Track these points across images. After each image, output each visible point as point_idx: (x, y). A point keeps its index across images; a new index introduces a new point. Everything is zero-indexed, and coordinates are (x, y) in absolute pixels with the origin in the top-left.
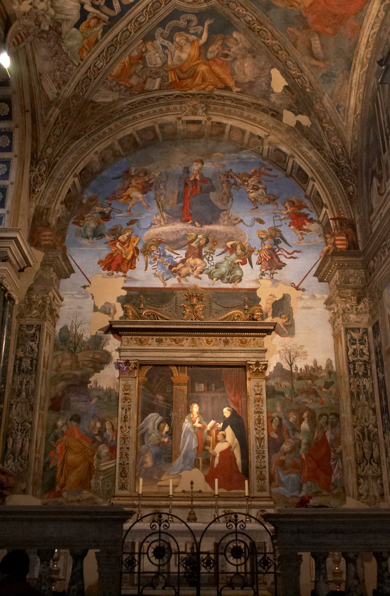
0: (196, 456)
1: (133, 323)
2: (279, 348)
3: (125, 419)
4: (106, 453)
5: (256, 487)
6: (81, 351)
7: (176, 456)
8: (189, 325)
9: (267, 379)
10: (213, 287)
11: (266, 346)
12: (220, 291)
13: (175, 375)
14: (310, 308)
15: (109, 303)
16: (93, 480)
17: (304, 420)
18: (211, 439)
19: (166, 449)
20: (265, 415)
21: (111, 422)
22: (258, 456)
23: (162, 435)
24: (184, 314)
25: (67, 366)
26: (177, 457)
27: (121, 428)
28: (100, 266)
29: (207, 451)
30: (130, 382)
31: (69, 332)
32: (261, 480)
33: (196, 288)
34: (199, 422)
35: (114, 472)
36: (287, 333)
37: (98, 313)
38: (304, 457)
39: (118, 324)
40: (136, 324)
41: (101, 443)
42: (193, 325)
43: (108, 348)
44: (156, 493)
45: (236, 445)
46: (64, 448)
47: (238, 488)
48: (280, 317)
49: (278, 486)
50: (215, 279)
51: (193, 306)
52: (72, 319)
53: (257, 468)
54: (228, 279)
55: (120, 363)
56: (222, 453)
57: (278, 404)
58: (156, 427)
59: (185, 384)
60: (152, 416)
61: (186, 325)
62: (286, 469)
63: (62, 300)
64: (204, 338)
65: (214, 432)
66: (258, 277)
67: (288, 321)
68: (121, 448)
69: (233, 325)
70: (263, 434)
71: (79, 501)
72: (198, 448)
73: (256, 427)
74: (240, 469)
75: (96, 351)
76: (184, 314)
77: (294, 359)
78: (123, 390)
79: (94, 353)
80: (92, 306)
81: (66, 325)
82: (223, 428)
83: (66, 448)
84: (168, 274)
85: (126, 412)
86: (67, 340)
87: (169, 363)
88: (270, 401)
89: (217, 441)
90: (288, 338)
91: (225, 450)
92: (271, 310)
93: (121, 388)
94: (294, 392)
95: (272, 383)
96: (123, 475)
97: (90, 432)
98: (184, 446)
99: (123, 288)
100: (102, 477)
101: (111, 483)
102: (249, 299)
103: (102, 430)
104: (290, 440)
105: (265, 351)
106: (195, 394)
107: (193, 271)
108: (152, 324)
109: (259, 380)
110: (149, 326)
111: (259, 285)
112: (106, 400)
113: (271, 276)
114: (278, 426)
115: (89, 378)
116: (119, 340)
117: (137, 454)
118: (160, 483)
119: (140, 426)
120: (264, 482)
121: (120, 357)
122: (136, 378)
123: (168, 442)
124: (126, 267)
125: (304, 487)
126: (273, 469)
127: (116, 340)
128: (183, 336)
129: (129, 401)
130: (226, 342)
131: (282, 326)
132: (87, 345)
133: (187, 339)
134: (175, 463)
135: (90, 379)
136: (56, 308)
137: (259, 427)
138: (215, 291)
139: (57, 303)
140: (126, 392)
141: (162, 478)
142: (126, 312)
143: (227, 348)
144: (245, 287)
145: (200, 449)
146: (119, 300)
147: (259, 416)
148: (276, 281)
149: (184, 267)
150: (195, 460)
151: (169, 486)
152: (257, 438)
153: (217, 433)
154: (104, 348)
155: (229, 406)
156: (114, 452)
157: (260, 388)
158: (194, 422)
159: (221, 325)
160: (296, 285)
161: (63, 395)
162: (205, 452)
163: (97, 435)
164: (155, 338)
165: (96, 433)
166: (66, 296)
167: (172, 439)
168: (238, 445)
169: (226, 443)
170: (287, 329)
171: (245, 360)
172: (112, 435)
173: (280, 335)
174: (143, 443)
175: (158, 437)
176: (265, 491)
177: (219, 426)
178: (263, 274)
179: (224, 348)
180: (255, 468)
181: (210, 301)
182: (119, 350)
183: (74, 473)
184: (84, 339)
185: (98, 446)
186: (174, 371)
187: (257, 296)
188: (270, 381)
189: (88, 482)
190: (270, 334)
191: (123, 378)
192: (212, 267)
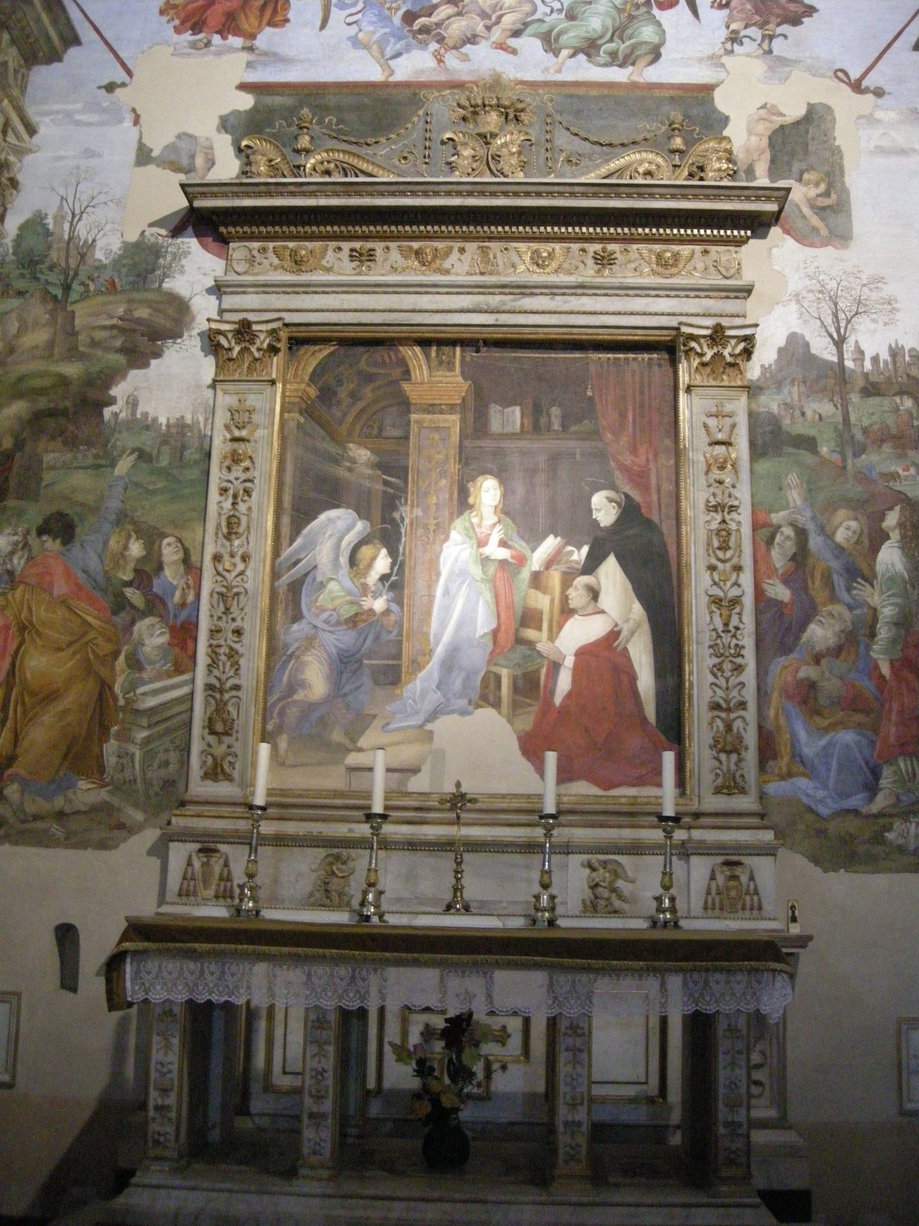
0: (489, 662)
1: (268, 190)
2: (796, 282)
3: (231, 527)
4: (160, 647)
5: (708, 779)
6: (86, 295)
7: (414, 661)
8: (470, 194)
9: (752, 390)
10: (560, 77)
11: (747, 277)
12: (581, 91)
13: (416, 374)
14: (903, 152)
15: (190, 136)
16: (112, 741)
17: (884, 536)
18: (543, 602)
19: (377, 637)
20: (743, 519)
21: (180, 540)
22: (719, 667)
23: (365, 587)
24: (451, 167)
25: (37, 347)
26: (417, 666)
27: (217, 558)
28: (164, 19)
29: (531, 644)
30: (252, 400)
31: (48, 233)
32: (728, 753)
33: (496, 83)
34: (503, 544)
35: (185, 716)
36: (824, 232)
37: (152, 168)
38: (885, 670)
39: (215, 195)
40: (281, 194)
41: (144, 614)
42: (482, 194)
43: (177, 284)
44: (336, 794)
45: (638, 626)
46: (14, 630)
47: (640, 782)
48: (800, 180)
49: (790, 775)
50: (565, 53)
51: (485, 139)
52: (62, 192)
53: (716, 706)
54: (613, 55)
55: (219, 332)
56: (583, 654)
57: (793, 478)
58: (344, 560)
59: (452, 408)
60: (330, 520)
61: (459, 194)
62: (818, 712)
63: (32, 130)
64: (522, 246)
65: (555, 579)
66: (718, 49)
67: (827, 194)
68: (215, 632)
69: (629, 196)
70: (736, 584)
71: (61, 815)
72: (495, 633)
73: (714, 561)
74: (650, 711)
75: (136, 295)
76: (451, 167)
77: (848, 322)
78: (227, 427)
79: (130, 301)
80: (134, 146)
81: (39, 212)
82: (591, 565)
83: (22, 628)
84: (400, 38)
85: (234, 504)
86: (43, 262)
87: (393, 333)
88: (764, 466)
89: (567, 611)
90: (829, 250)
91: (597, 644)
92: (767, 155)
93: (222, 418)
94: (853, 437)
95: (771, 403)
96: (219, 727)
97: (109, 580)
98: (443, 625)
99: (244, 87)
100: (144, 734)
101: (173, 757)
102: (686, 116)
103: (146, 569)
104: (837, 608)
105: (747, 291)
106: (487, 444)
107: (488, 28)
108: (337, 194)
109: (725, 392)
110: (323, 202)
111: (722, 75)
112: (164, 462)
113: (765, 46)
114: (793, 558)
115: (108, 387)
116: (219, 256)
117: (272, 651)
118: (353, 759)
119: (286, 553)
120: (740, 760)
121: (221, 312)
122: (273, 382)
123: (387, 612)
124: (254, 22)
125: (886, 781)
126: (772, 713)
127: (208, 256)
128: (450, 237)
129: (247, 463)
130: (604, 261)
131: (806, 210)
132: (107, 275)
133: (462, 250)
134: (410, 686)
135: (114, 391)
136: (12, 158)
137: (723, 561)
138: (567, 91)
139: (17, 143)
140: (237, 433)
141: (362, 743)
142: (249, 164)
143: (608, 278)
144: (672, 81)
145: (501, 636)
146: (225, 124)
147: (724, 521)
148: (783, 61)
149: (459, 14)
150: (485, 680)
151: (371, 769)
152: (716, 601)
153: (567, 582)
154: (168, 285)
155: (613, 487)
156: (190, 644)
157: (728, 421)
158: (482, 543)
159: (585, 195)
160: (854, 75)
161: (19, 445)
162: (522, 649)
163: (129, 584)
164: (346, 246)
165: (127, 576)
166: (47, 120)
167: (400, 603)
168: (646, 628)
169: (599, 618)
170: (823, 220)
171: (673, 322)
172: (182, 583)
173: (802, 239)
174: (297, 616)
175: (349, 593)
176: (743, 791)
177: (575, 557)
178: (735, 38)
179: (598, 280)
180: (705, 707)
181: (548, 121)
182: (218, 289)
183: (47, 718)
184: (99, 255)
185: (133, 623)
186: (412, 364)
187: (715, 110)
188: (763, 399)
189: (96, 750)
190: (764, 236)
191: (230, 387)
192: (555, 16)
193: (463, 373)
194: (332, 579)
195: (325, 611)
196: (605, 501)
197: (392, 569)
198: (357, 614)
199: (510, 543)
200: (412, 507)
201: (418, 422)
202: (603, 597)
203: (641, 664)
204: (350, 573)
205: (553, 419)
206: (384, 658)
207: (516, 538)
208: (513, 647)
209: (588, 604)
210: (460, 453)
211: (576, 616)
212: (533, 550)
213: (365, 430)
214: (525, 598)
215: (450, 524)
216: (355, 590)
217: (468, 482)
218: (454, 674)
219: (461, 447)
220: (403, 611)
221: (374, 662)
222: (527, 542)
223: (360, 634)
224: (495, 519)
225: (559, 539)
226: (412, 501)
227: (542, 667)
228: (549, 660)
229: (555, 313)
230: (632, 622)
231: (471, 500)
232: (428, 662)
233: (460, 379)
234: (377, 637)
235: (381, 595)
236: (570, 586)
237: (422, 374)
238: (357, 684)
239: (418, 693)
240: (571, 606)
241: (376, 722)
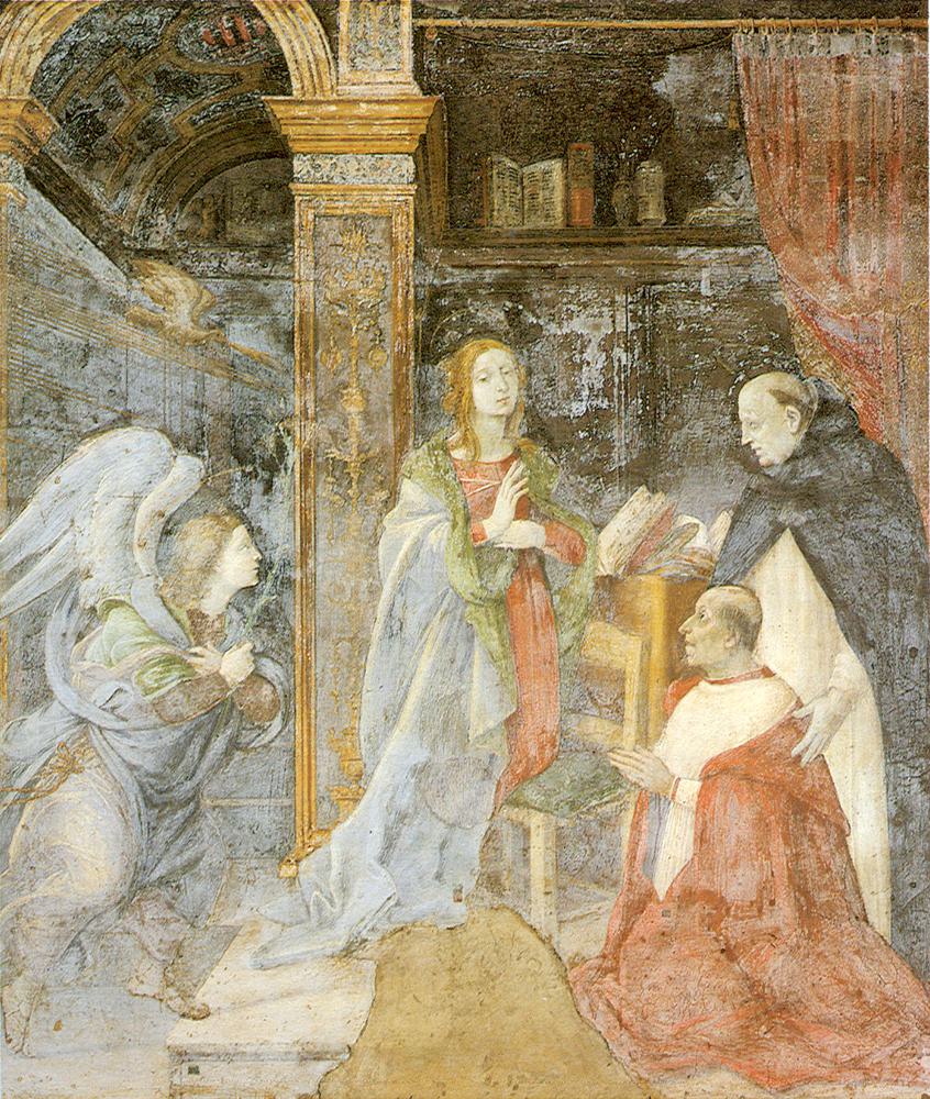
34: (524, 510)
45: (850, 703)
82: (738, 564)
89: (681, 676)
118: (185, 1033)
123: (257, 676)
141: (204, 996)
168: (867, 708)
195: (103, 681)
202: (766, 637)
211: (703, 684)
236: (691, 610)
238: (188, 855)
240: (691, 661)
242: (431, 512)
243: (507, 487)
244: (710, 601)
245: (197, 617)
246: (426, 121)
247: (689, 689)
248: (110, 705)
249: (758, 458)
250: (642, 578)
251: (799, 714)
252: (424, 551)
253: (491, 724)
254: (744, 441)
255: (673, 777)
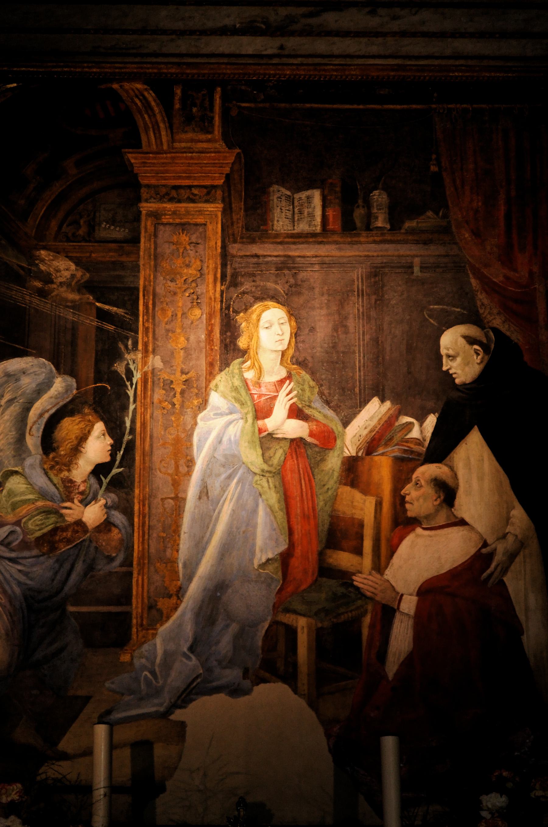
0: (275, 607)
7: (151, 607)
19: (90, 568)
45: (522, 545)
134: (146, 647)
145: (295, 563)
162: (331, 584)
175: (43, 495)
177: (415, 433)
193: (225, 137)
194: (16, 473)
196: (462, 341)
197: (113, 455)
198: (55, 531)
199: (307, 411)
200: (146, 351)
201: (156, 215)
203: (527, 609)
204: (42, 463)
205: (375, 210)
206: (99, 602)
207: (318, 404)
208: (316, 580)
209: (437, 511)
210: (224, 265)
211: (419, 530)
212: (346, 423)
213: (64, 228)
214: (335, 498)
215: (208, 381)
216: (52, 489)
217: (237, 312)
218: (218, 627)
219: (225, 255)
220: (132, 524)
221: (84, 609)
222: (336, 409)
223: (60, 562)
224: (283, 373)
225: (388, 404)
226: (146, 345)
227: (366, 612)
228: (377, 603)
229: (378, 35)
230: (510, 539)
231: (242, 343)
232: (176, 608)
233: (220, 145)
234: (90, 568)
235: (95, 498)
236: (408, 480)
237: (158, 137)
239: (158, 661)
240: (409, 514)
241: (89, 709)
242: (231, 413)
243: (282, 399)
244: (423, 473)
245: (69, 484)
246: (230, 166)
247: (408, 533)
248: (6, 541)
249: (454, 379)
250: (376, 458)
251: (484, 551)
252: (225, 439)
253: (270, 556)
254: (445, 368)
255: (398, 593)
